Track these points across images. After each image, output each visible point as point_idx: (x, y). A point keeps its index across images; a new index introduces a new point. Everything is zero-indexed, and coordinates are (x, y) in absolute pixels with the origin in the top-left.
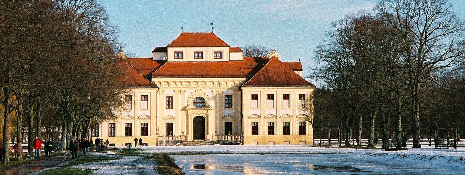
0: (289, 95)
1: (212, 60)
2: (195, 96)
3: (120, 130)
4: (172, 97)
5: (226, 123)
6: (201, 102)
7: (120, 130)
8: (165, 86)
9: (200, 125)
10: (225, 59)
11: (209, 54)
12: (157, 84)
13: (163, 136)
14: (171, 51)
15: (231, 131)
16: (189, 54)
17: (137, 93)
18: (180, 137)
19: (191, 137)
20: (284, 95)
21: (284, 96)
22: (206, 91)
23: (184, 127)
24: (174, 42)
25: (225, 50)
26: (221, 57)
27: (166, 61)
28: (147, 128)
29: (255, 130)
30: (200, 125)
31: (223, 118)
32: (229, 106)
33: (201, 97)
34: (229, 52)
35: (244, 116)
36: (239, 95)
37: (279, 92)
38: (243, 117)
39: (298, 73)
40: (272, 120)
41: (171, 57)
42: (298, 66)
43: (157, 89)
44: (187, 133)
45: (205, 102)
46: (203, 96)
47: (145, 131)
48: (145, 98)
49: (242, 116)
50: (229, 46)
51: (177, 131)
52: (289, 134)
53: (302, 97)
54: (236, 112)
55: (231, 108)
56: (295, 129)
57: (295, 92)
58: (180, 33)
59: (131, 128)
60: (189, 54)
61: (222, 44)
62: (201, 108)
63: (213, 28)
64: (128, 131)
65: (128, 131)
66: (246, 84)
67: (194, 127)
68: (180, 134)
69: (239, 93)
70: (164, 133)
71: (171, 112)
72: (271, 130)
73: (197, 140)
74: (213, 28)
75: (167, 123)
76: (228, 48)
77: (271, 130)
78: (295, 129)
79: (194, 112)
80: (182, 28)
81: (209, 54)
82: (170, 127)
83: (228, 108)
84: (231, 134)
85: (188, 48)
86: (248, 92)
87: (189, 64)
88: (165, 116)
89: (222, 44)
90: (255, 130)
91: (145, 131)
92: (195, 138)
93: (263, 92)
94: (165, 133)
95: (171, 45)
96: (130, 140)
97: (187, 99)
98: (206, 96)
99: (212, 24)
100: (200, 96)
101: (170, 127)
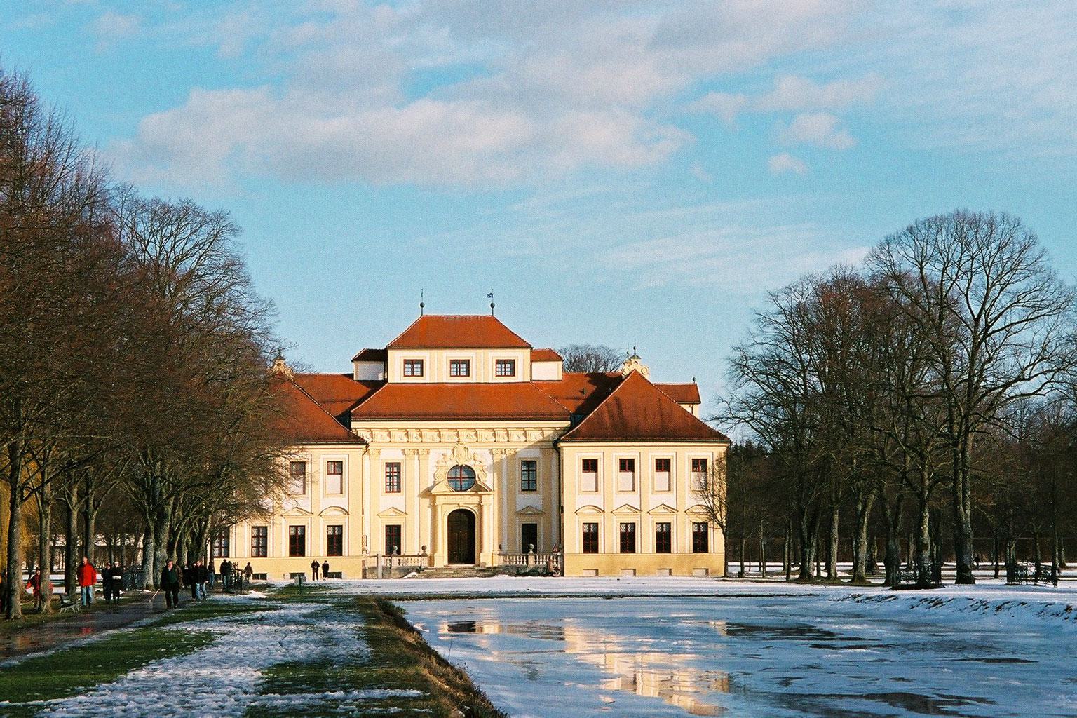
0: (669, 460)
1: (492, 379)
2: (451, 464)
3: (279, 541)
4: (398, 465)
5: (523, 525)
6: (465, 478)
7: (279, 541)
8: (382, 441)
9: (463, 531)
10: (521, 376)
11: (484, 366)
12: (364, 434)
13: (377, 556)
14: (396, 358)
15: (535, 544)
16: (437, 366)
17: (318, 457)
18: (416, 558)
19: (441, 559)
20: (657, 460)
21: (657, 464)
23: (425, 535)
24: (403, 336)
25: (521, 356)
26: (513, 373)
27: (385, 381)
28: (340, 537)
29: (591, 542)
30: (463, 531)
31: (516, 513)
32: (530, 485)
33: (466, 465)
34: (531, 361)
35: (565, 509)
36: (555, 461)
37: (646, 453)
38: (562, 512)
39: (689, 410)
40: (629, 519)
41: (396, 373)
42: (690, 394)
43: (364, 446)
44: (434, 550)
45: (475, 478)
46: (471, 464)
47: (335, 544)
48: (337, 467)
49: (561, 508)
50: (530, 347)
51: (410, 544)
52: (670, 552)
53: (699, 464)
54: (547, 500)
55: (536, 490)
56: (682, 539)
57: (682, 454)
58: (417, 317)
59: (302, 538)
60: (437, 366)
61: (515, 342)
62: (465, 491)
63: (492, 306)
64: (297, 545)
65: (297, 545)
66: (571, 435)
67: (448, 537)
68: (418, 551)
69: (555, 456)
70: (380, 550)
71: (395, 500)
72: (628, 542)
73: (456, 566)
75: (387, 526)
76: (529, 350)
77: (628, 542)
78: (682, 539)
79: (450, 499)
80: (422, 305)
81: (484, 366)
82: (394, 536)
83: (529, 490)
84: (535, 551)
85: (435, 352)
86: (574, 454)
87: (438, 388)
88: (381, 510)
89: (515, 342)
90: (591, 542)
91: (335, 544)
92: (451, 560)
93: (609, 453)
94: (381, 549)
95: (397, 345)
96: (302, 565)
97: (432, 470)
98: (477, 463)
99: (491, 295)
100: (464, 463)
101: (394, 536)
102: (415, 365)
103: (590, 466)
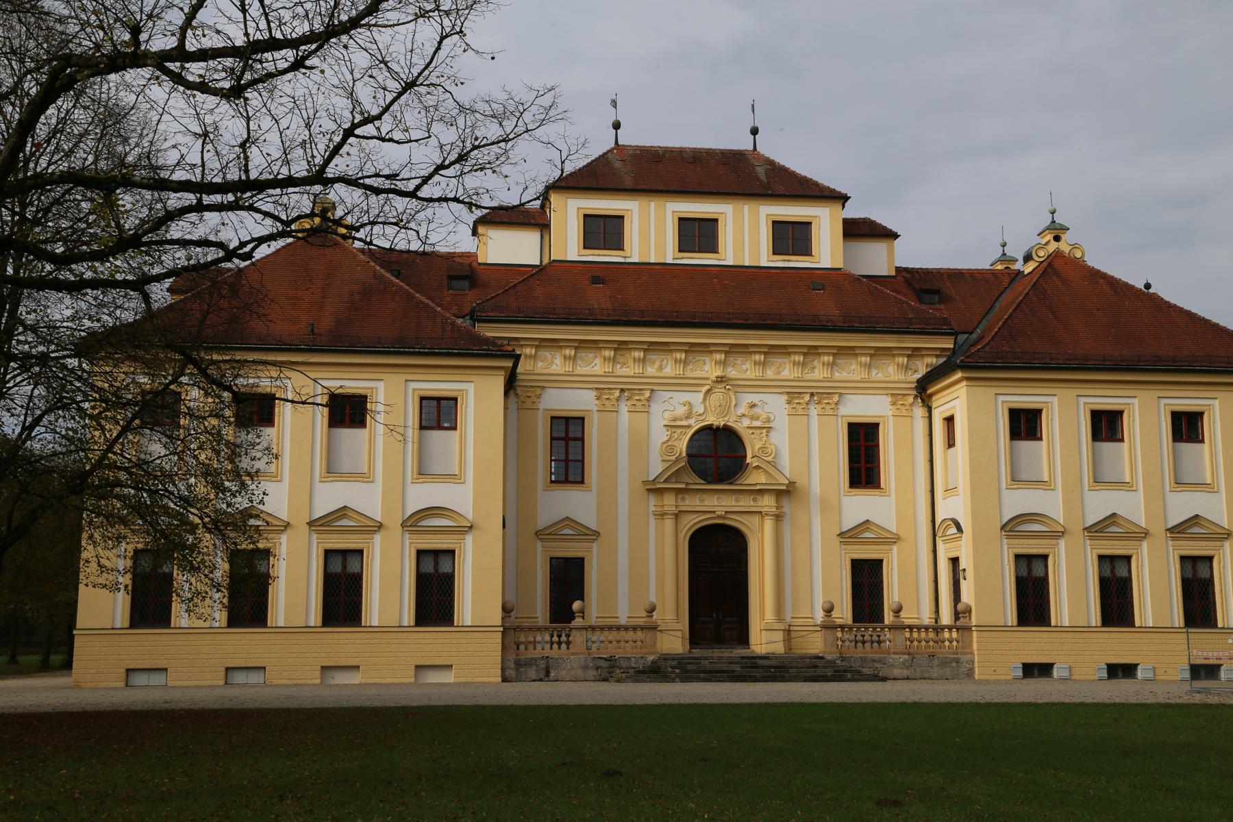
1: (764, 257)
11: (745, 234)
16: (651, 231)
22: (755, 398)
23: (640, 578)
46: (741, 426)
50: (843, 199)
60: (651, 231)
63: (755, 131)
69: (919, 412)
71: (576, 504)
74: (755, 131)
79: (691, 502)
80: (617, 126)
92: (696, 636)
101: (568, 580)
102: (603, 231)
103: (1025, 425)
